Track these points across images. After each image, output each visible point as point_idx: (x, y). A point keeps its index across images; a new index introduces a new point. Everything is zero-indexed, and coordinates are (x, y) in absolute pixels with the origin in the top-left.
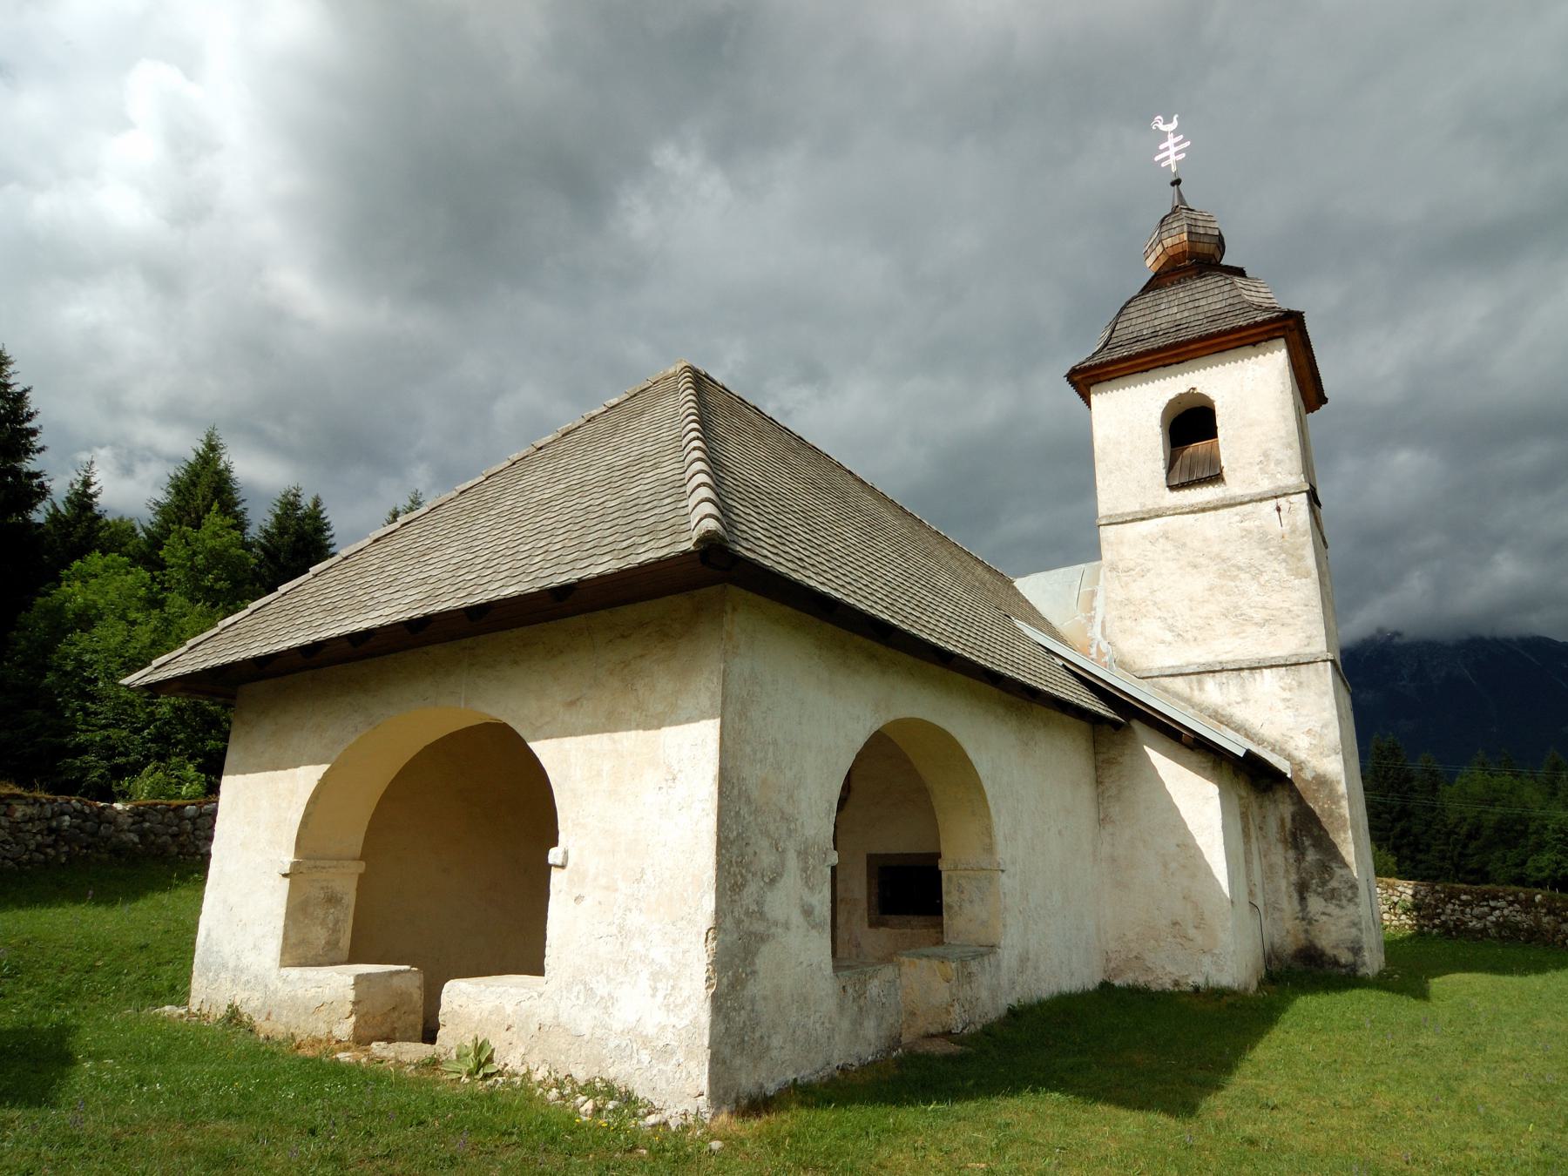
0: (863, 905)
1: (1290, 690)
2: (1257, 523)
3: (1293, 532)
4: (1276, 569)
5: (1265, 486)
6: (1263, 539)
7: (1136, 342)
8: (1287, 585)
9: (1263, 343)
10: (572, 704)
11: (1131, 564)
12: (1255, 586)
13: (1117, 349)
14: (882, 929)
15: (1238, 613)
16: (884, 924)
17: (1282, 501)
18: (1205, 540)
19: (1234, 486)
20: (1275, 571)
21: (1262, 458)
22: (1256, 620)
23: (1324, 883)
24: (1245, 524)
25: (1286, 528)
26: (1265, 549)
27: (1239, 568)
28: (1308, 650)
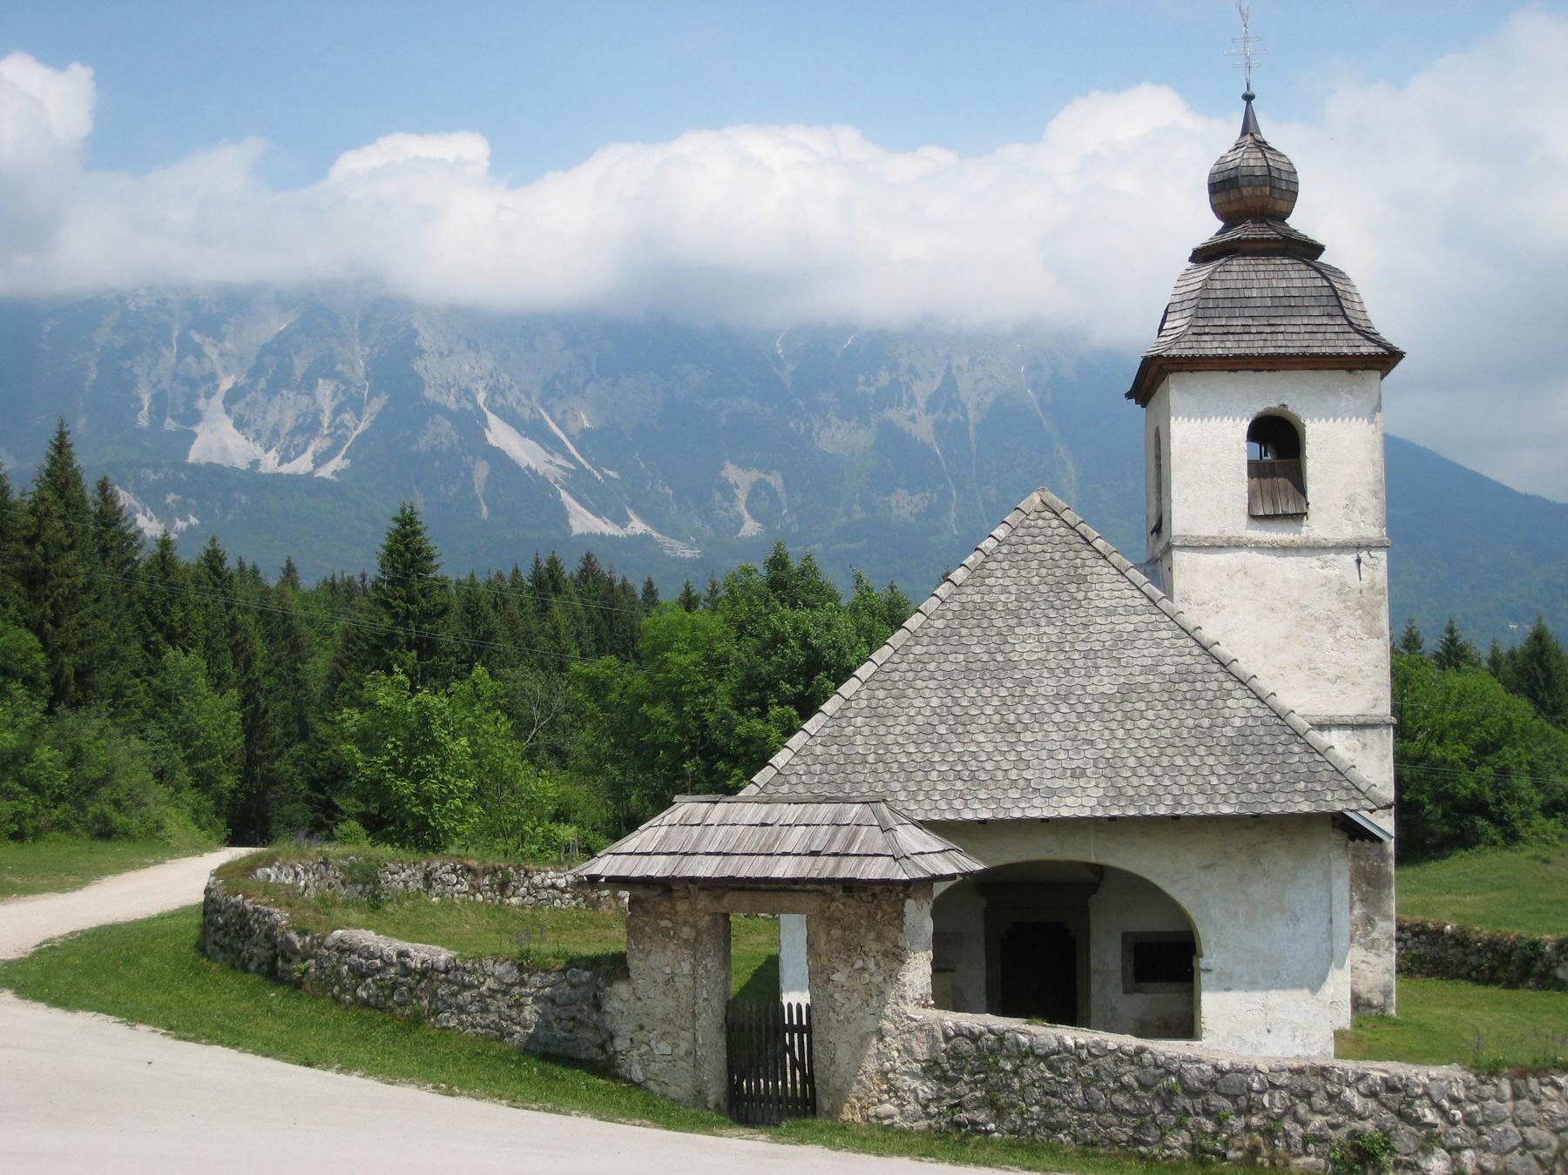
0: (1119, 975)
1: (1354, 751)
2: (1337, 572)
3: (1372, 588)
4: (1352, 624)
5: (1348, 533)
6: (1342, 591)
8: (1362, 643)
9: (1360, 372)
10: (1207, 867)
11: (1206, 597)
12: (1330, 640)
13: (1206, 338)
14: (1137, 995)
15: (1312, 666)
16: (1138, 991)
17: (1364, 555)
18: (1285, 581)
19: (1317, 527)
20: (1350, 627)
21: (1347, 502)
22: (1327, 676)
23: (1367, 934)
24: (1325, 571)
25: (1365, 583)
26: (1344, 602)
27: (1317, 619)
28: (1374, 712)
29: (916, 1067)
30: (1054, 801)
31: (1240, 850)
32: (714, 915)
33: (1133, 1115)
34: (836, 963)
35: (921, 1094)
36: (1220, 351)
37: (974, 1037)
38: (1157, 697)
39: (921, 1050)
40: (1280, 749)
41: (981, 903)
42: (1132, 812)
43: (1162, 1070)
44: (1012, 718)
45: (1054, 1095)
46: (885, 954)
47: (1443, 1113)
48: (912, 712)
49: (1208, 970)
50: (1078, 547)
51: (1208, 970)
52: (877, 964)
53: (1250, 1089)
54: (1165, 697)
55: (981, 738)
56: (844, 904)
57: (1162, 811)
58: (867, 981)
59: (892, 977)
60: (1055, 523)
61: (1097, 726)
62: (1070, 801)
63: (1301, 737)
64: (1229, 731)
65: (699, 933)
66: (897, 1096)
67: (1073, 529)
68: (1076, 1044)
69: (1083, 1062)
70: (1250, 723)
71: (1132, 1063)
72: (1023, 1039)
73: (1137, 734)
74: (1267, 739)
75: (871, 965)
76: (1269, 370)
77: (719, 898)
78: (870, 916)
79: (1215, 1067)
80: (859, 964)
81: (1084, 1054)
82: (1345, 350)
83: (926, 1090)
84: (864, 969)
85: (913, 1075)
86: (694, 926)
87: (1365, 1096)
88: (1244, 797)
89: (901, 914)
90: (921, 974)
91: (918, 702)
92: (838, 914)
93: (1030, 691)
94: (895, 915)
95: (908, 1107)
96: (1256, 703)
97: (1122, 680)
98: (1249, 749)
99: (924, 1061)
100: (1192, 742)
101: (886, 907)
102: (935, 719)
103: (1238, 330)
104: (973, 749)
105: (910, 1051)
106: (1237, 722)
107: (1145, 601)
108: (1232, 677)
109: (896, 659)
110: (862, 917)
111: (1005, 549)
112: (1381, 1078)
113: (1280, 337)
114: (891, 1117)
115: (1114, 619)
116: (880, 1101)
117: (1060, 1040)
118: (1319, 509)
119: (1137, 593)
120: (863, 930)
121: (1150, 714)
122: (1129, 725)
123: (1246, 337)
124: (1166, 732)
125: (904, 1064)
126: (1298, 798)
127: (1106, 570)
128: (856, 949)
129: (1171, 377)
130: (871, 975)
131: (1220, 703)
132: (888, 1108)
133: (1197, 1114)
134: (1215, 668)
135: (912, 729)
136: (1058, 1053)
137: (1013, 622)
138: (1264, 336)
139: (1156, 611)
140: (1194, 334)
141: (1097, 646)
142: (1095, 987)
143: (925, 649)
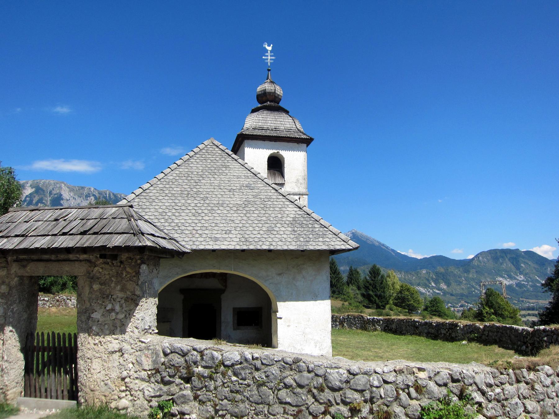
0: (231, 323)
7: (262, 129)
10: (280, 274)
13: (256, 130)
14: (238, 331)
16: (239, 329)
29: (144, 374)
30: (218, 243)
31: (293, 267)
32: (21, 278)
33: (293, 406)
34: (94, 305)
35: (147, 393)
36: (261, 134)
37: (184, 354)
38: (259, 206)
39: (147, 364)
40: (310, 226)
41: (182, 297)
42: (252, 247)
43: (312, 374)
44: (200, 211)
45: (237, 392)
46: (127, 299)
47: (483, 393)
48: (157, 207)
49: (281, 318)
50: (225, 157)
51: (281, 318)
52: (121, 306)
53: (372, 386)
54: (263, 206)
55: (187, 218)
56: (102, 268)
57: (265, 247)
58: (114, 317)
59: (129, 314)
60: (217, 149)
61: (235, 215)
62: (226, 243)
63: (318, 222)
64: (289, 219)
65: (11, 288)
66: (132, 395)
67: (223, 151)
68: (253, 357)
69: (257, 369)
70: (297, 216)
71: (291, 370)
72: (216, 354)
73: (252, 218)
74: (305, 222)
75: (117, 308)
76: (274, 142)
77: (24, 267)
78: (119, 275)
79: (349, 372)
80: (109, 307)
81: (258, 363)
82: (297, 136)
83: (150, 390)
84: (113, 310)
85: (143, 380)
86: (8, 285)
87: (440, 385)
88: (298, 243)
89: (138, 273)
90: (150, 313)
91: (160, 204)
92: (98, 275)
93: (207, 202)
94: (134, 274)
95: (138, 402)
96: (298, 209)
97: (244, 199)
98: (298, 226)
99: (150, 370)
100: (275, 222)
101: (128, 269)
102: (167, 211)
103: (266, 129)
104: (183, 221)
105: (140, 363)
106: (292, 216)
107: (252, 174)
108: (288, 200)
109: (152, 188)
110: (113, 276)
111: (198, 156)
112: (449, 374)
113: (278, 131)
114: (126, 408)
115: (240, 179)
116: (120, 398)
117: (242, 355)
118: (288, 183)
119: (249, 172)
120: (113, 285)
121: (257, 212)
122: (248, 215)
123: (268, 131)
124: (264, 218)
125: (136, 372)
126: (320, 244)
127: (237, 164)
128: (108, 296)
129: (245, 141)
130: (117, 313)
131: (284, 209)
132: (124, 402)
133: (338, 404)
134: (281, 197)
135: (156, 214)
136: (241, 363)
137: (201, 178)
138: (273, 131)
139: (257, 178)
140: (253, 129)
141: (234, 188)
142: (223, 328)
143: (164, 186)
